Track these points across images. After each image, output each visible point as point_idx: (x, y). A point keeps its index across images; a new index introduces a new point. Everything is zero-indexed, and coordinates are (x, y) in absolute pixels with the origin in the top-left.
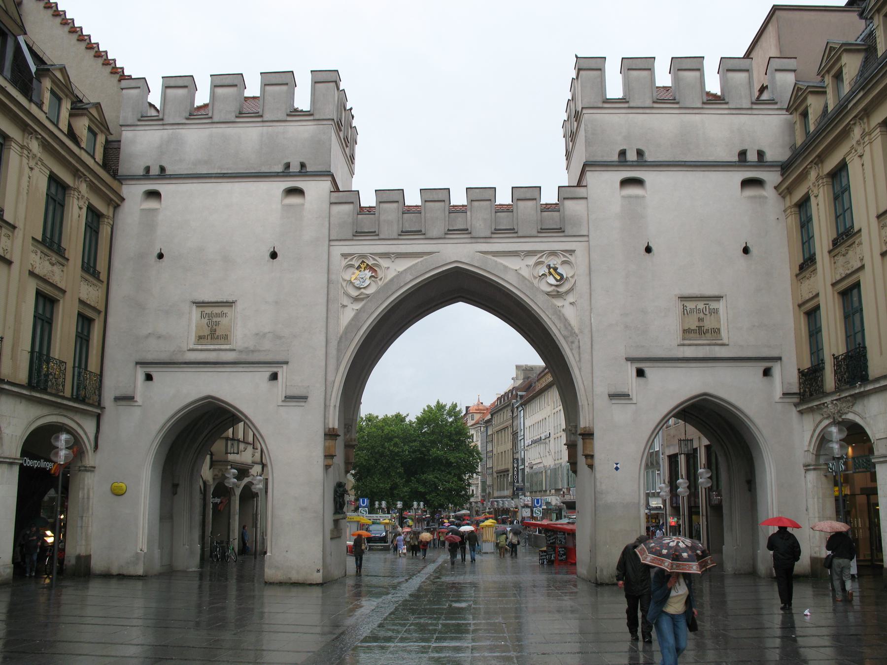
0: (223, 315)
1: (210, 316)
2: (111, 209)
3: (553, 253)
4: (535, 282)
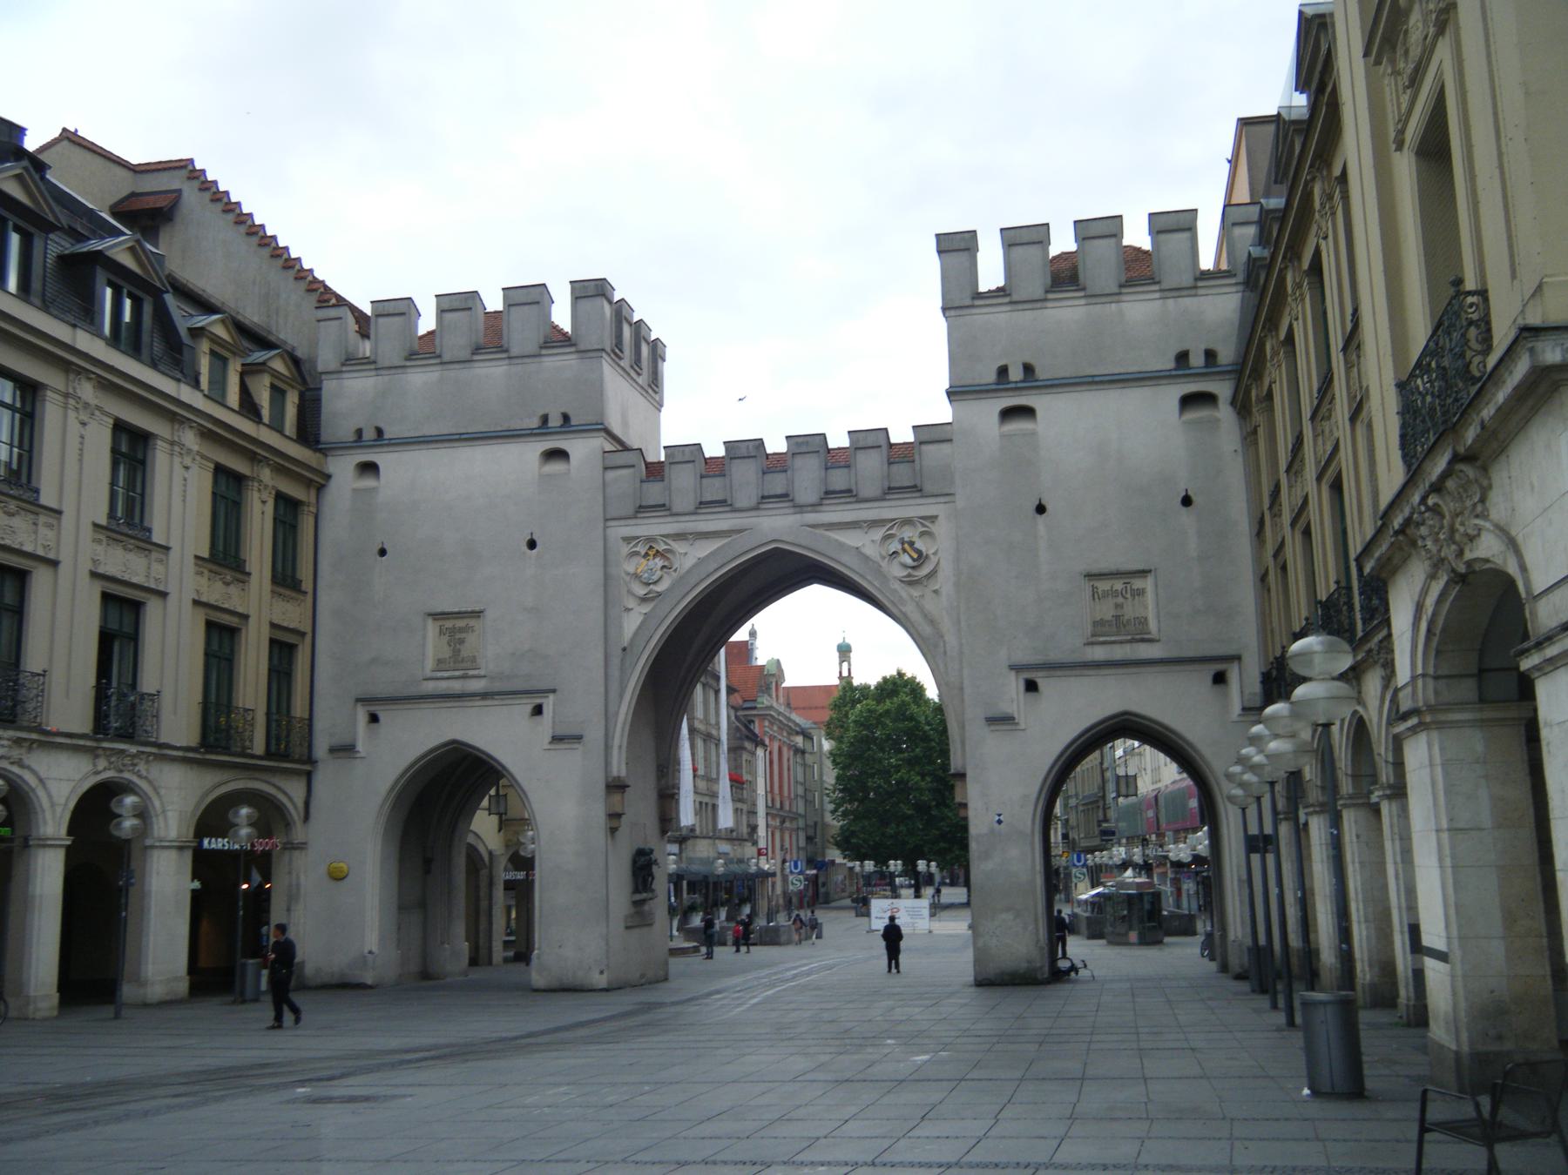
1: (453, 631)
2: (313, 493)
3: (908, 522)
4: (884, 564)
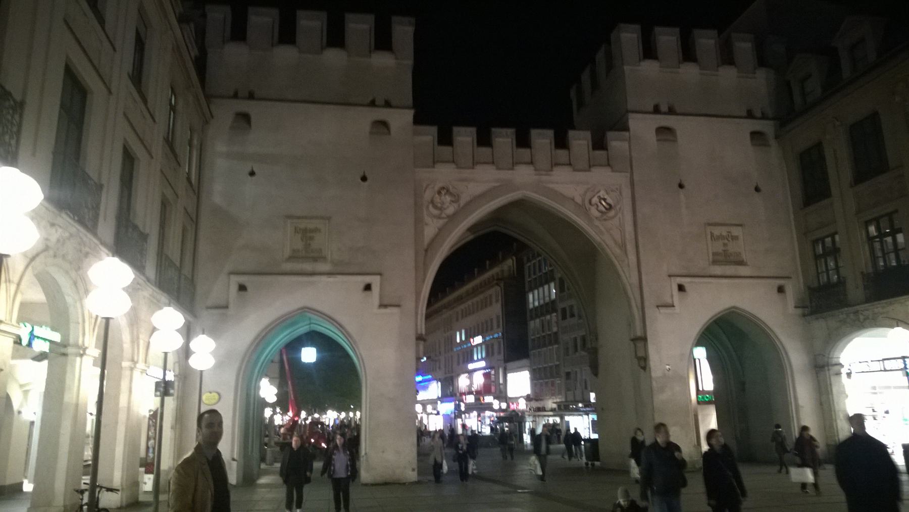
0: (316, 230)
1: (305, 231)
